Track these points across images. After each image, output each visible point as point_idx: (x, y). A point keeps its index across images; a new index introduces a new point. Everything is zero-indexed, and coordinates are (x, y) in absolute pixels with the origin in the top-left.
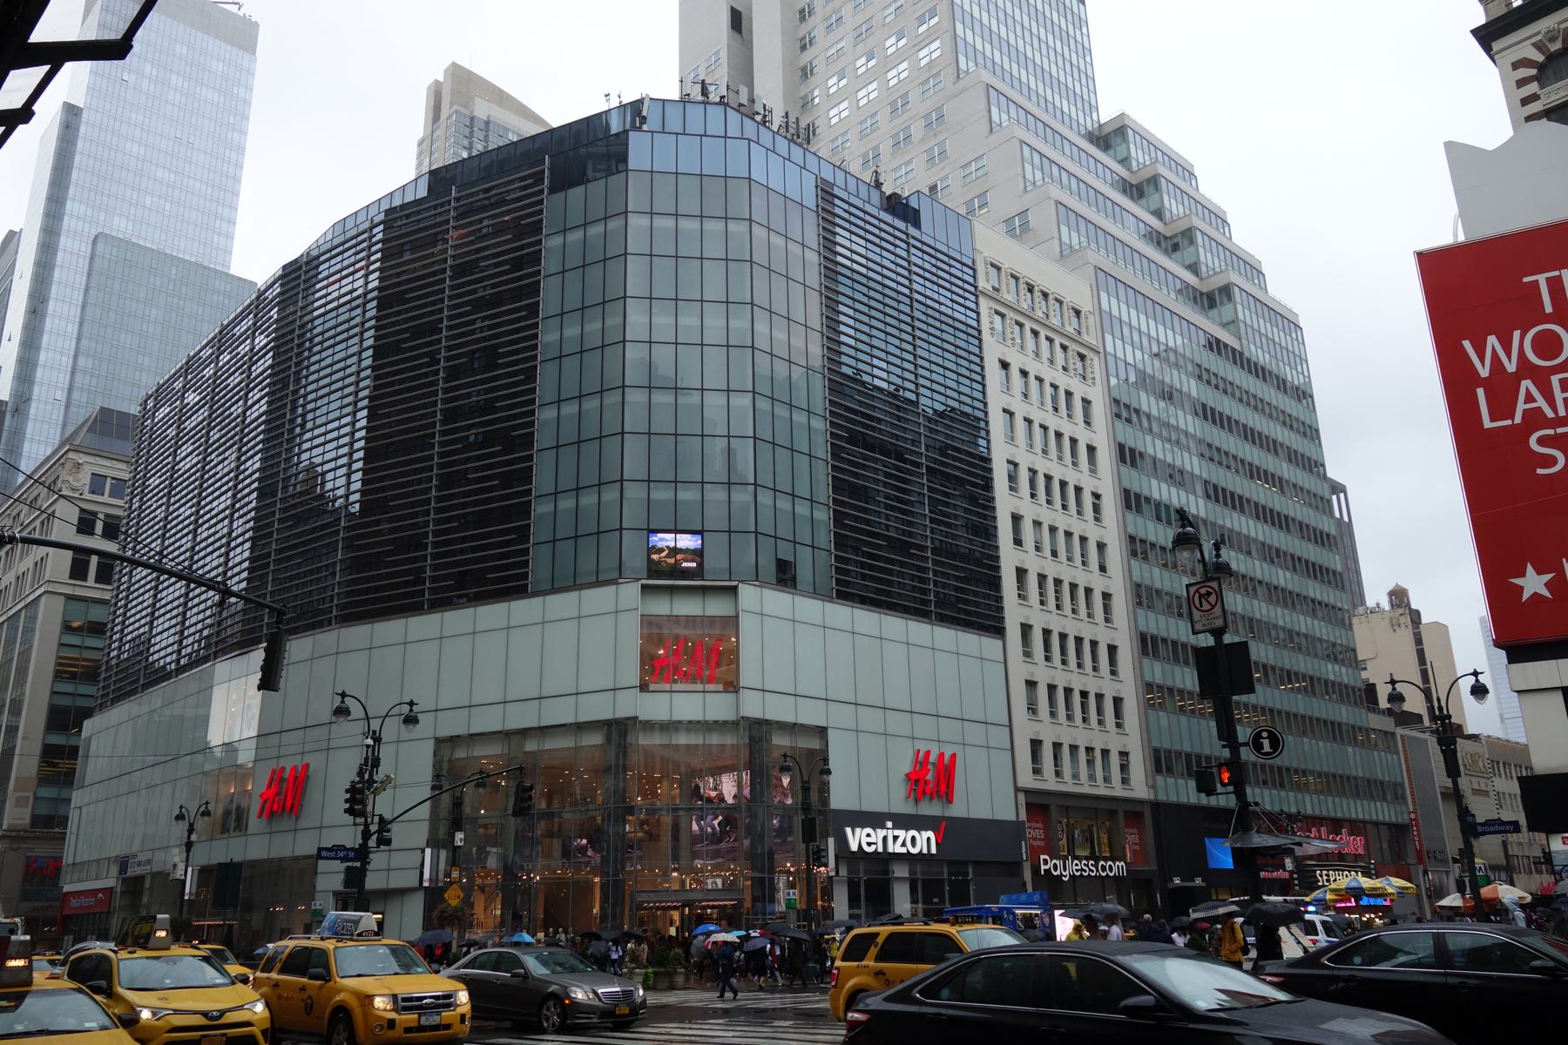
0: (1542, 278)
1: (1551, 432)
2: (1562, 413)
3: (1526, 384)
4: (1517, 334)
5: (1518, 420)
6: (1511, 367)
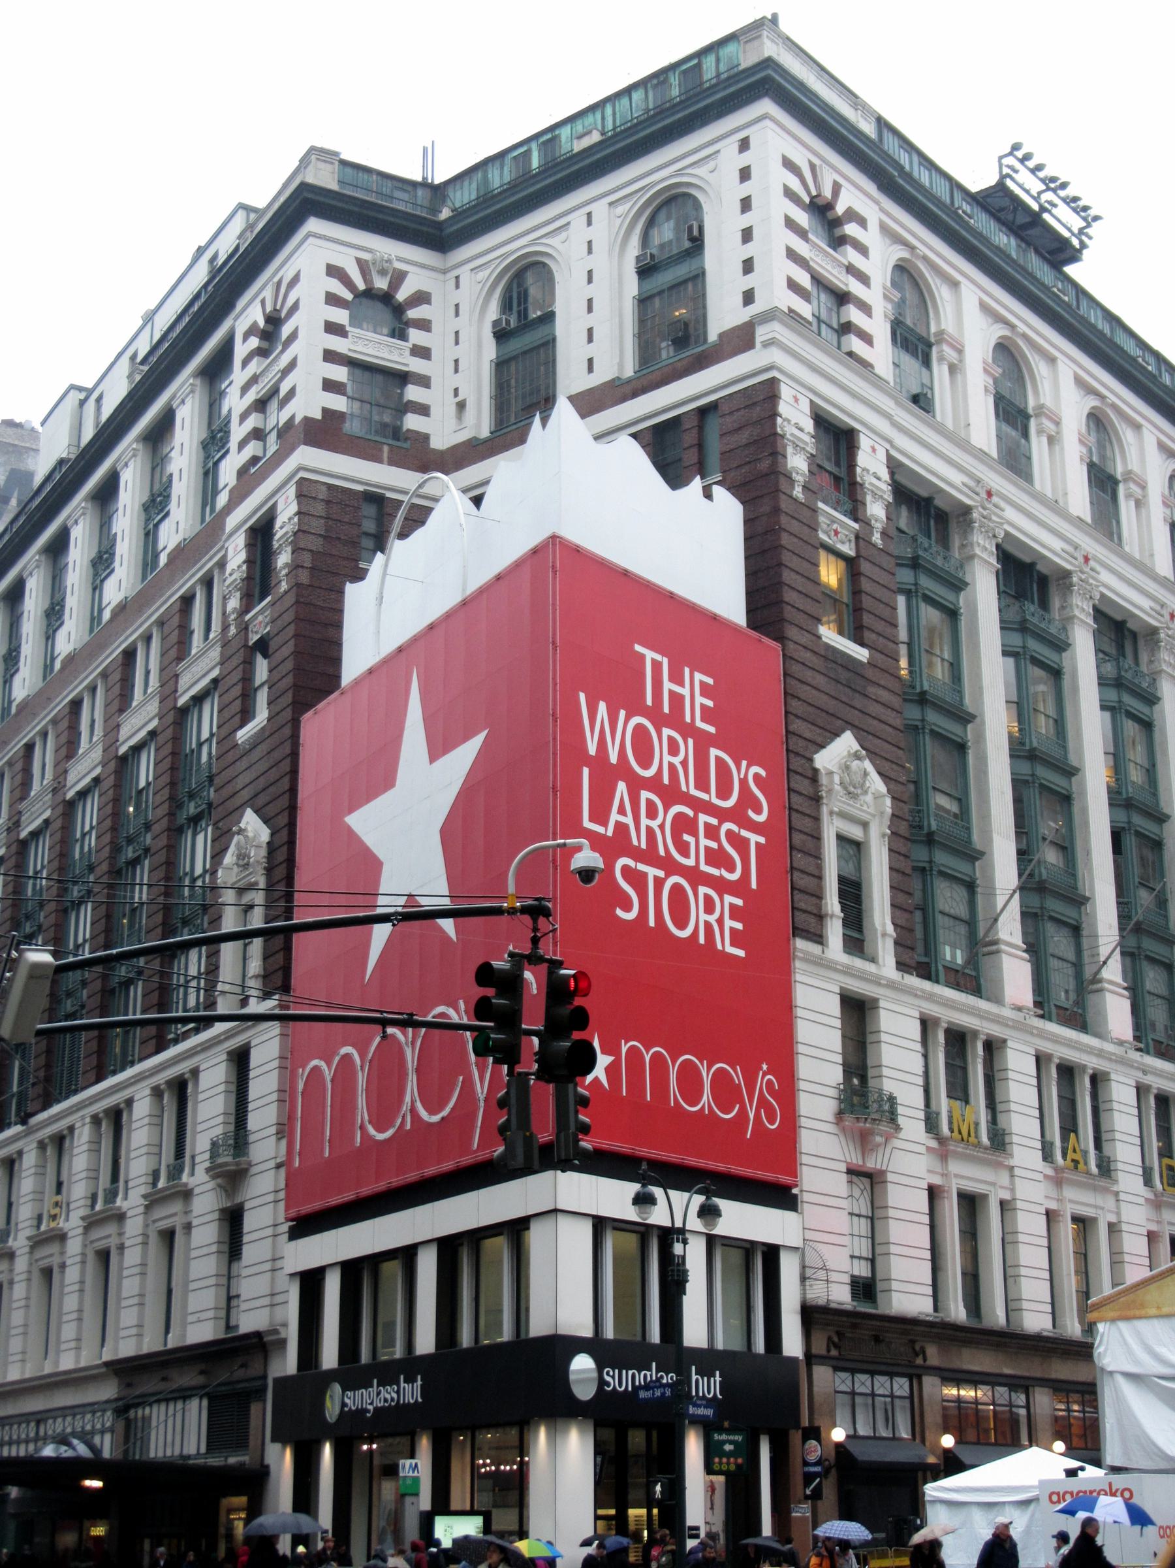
0: (650, 655)
1: (631, 863)
2: (644, 846)
3: (622, 787)
4: (622, 713)
5: (610, 833)
6: (614, 759)
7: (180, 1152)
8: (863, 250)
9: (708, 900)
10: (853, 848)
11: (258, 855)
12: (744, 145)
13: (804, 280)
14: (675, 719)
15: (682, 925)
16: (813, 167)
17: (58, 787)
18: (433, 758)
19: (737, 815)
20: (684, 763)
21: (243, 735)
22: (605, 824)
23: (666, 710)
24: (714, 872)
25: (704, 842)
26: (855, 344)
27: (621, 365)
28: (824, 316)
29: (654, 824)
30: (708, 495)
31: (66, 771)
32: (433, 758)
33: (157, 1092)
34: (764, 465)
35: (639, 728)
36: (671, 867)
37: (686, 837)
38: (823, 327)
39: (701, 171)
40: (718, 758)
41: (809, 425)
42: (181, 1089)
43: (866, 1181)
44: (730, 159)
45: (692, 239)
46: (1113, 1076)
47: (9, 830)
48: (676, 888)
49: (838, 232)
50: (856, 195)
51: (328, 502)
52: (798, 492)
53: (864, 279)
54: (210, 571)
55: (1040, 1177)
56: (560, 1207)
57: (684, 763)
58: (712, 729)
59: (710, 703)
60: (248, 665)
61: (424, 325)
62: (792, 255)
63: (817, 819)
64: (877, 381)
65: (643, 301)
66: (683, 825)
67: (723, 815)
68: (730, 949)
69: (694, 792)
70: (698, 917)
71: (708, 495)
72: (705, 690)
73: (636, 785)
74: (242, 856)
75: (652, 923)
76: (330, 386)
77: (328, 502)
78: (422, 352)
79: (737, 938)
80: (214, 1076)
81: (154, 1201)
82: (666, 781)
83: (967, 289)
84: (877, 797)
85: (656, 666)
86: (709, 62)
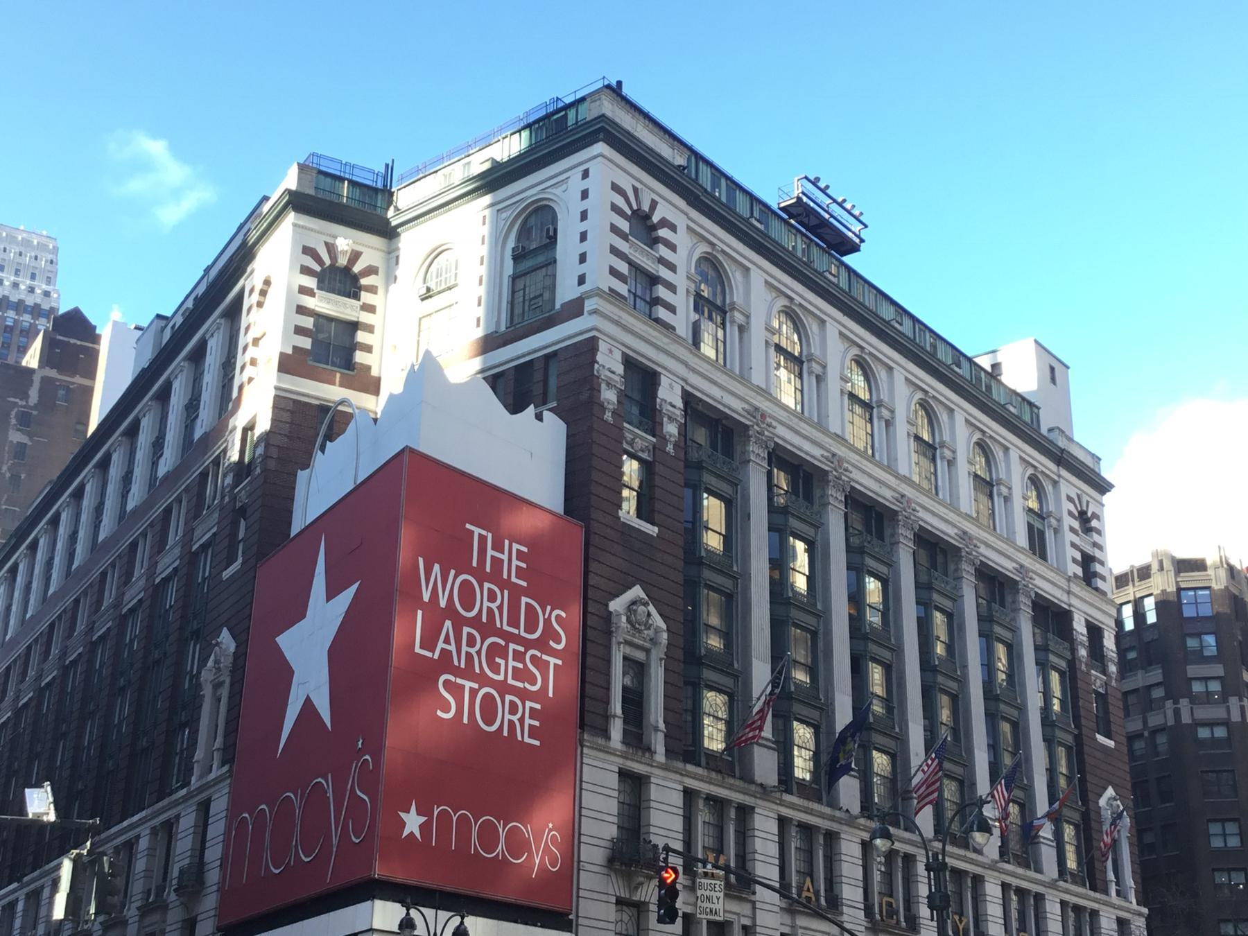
0: (477, 531)
1: (452, 678)
2: (463, 666)
3: (448, 624)
4: (453, 572)
5: (436, 657)
6: (443, 604)
7: (165, 879)
8: (673, 247)
9: (512, 703)
10: (637, 669)
11: (227, 662)
12: (586, 174)
13: (623, 268)
14: (495, 576)
15: (490, 722)
16: (636, 190)
17: (117, 605)
18: (328, 600)
19: (541, 644)
20: (500, 608)
21: (226, 574)
22: (433, 651)
23: (488, 569)
24: (520, 685)
25: (511, 663)
26: (662, 313)
27: (498, 323)
28: (639, 293)
29: (473, 651)
30: (539, 417)
31: (123, 594)
32: (328, 600)
33: (154, 832)
34: (584, 397)
35: (465, 582)
36: (483, 680)
37: (498, 660)
38: (638, 300)
39: (558, 191)
40: (527, 604)
41: (620, 369)
42: (169, 828)
43: (635, 911)
44: (576, 183)
45: (549, 237)
46: (843, 836)
47: (86, 634)
48: (487, 695)
49: (654, 235)
50: (670, 208)
51: (292, 412)
52: (608, 416)
53: (672, 267)
54: (219, 456)
55: (777, 909)
56: (375, 927)
57: (500, 608)
58: (524, 584)
59: (524, 565)
60: (235, 526)
61: (372, 289)
62: (614, 251)
63: (608, 648)
64: (678, 339)
65: (514, 278)
66: (494, 651)
67: (529, 645)
68: (527, 740)
69: (506, 628)
70: (503, 716)
71: (539, 417)
72: (521, 556)
73: (459, 622)
74: (217, 662)
75: (465, 721)
76: (299, 330)
77: (292, 412)
78: (370, 309)
79: (533, 732)
80: (187, 822)
81: (145, 911)
82: (484, 620)
83: (755, 274)
84: (658, 631)
85: (482, 539)
86: (571, 114)
